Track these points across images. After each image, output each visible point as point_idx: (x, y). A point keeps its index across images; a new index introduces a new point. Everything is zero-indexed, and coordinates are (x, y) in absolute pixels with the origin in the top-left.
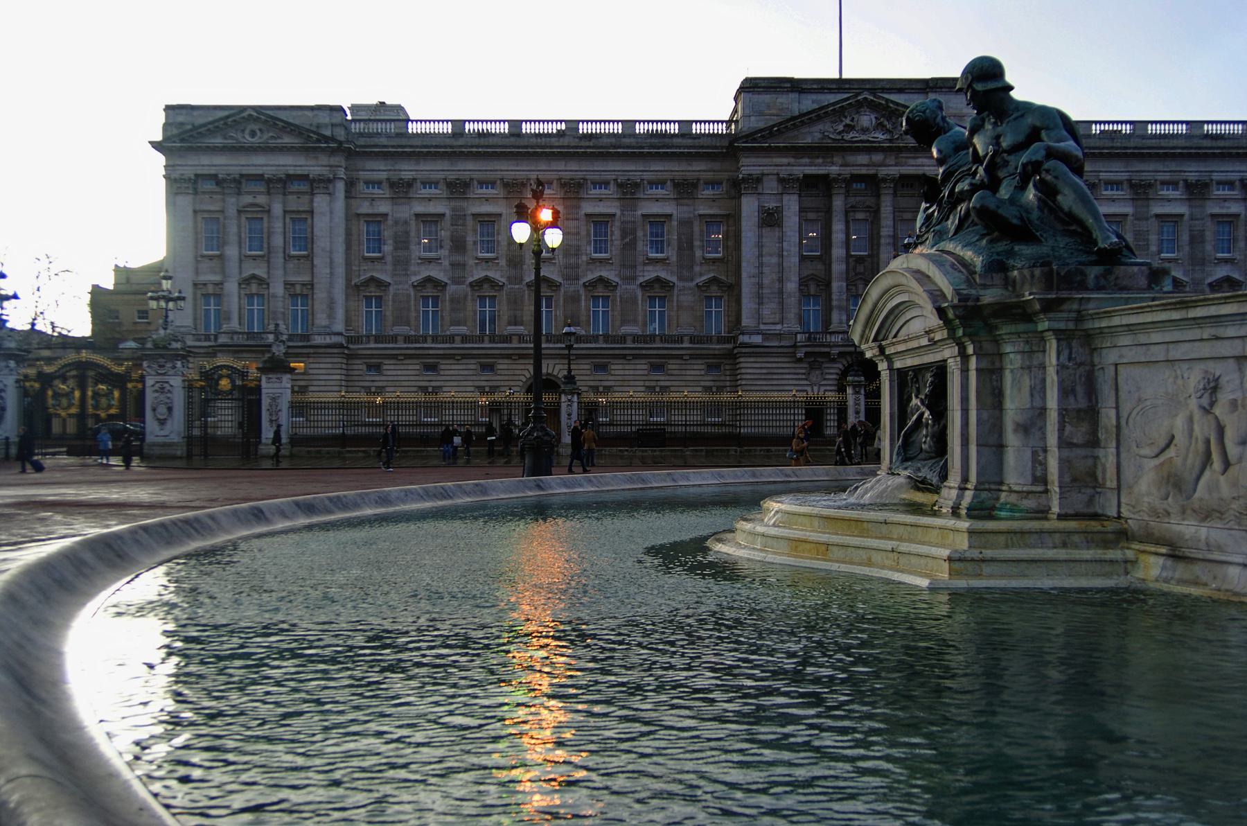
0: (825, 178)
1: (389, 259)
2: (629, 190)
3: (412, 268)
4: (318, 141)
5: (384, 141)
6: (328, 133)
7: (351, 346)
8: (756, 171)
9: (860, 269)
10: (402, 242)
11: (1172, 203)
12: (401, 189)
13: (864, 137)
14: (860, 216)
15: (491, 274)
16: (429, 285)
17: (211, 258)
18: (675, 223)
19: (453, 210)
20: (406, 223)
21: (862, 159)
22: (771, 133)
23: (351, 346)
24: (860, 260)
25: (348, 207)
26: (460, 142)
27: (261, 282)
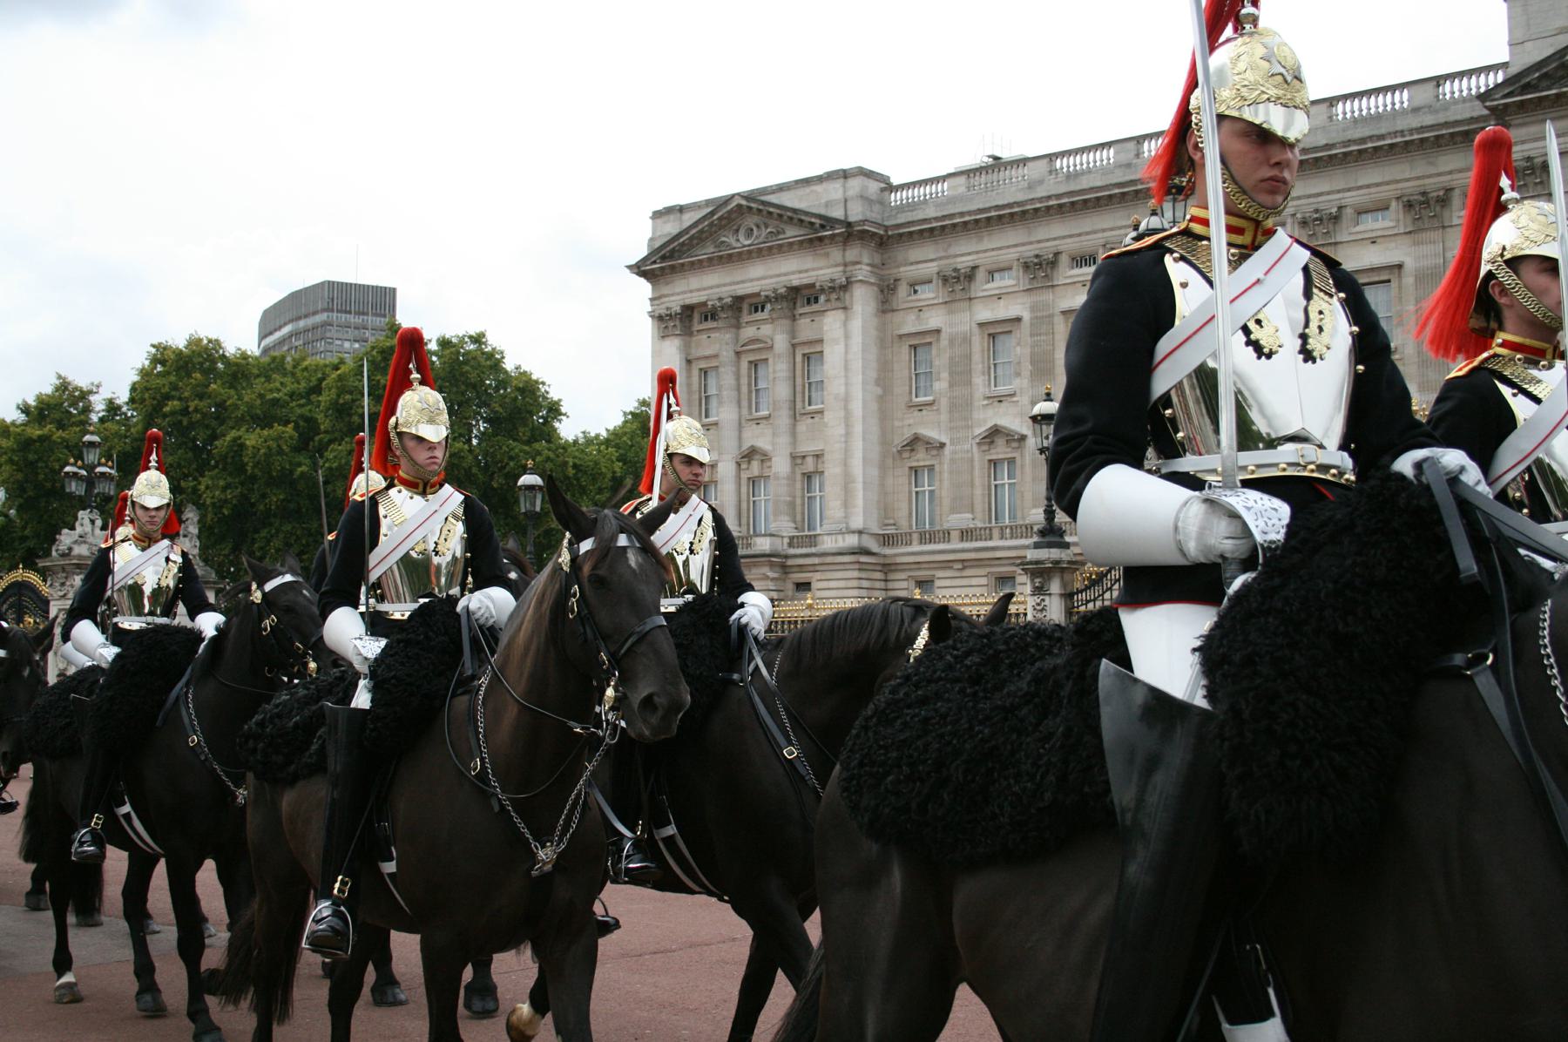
1: (944, 403)
3: (976, 415)
4: (823, 227)
5: (931, 212)
6: (837, 213)
7: (888, 551)
10: (961, 374)
12: (959, 282)
16: (1000, 441)
18: (1409, 280)
19: (1033, 309)
20: (966, 340)
23: (888, 551)
25: (882, 328)
26: (1041, 192)
27: (765, 458)
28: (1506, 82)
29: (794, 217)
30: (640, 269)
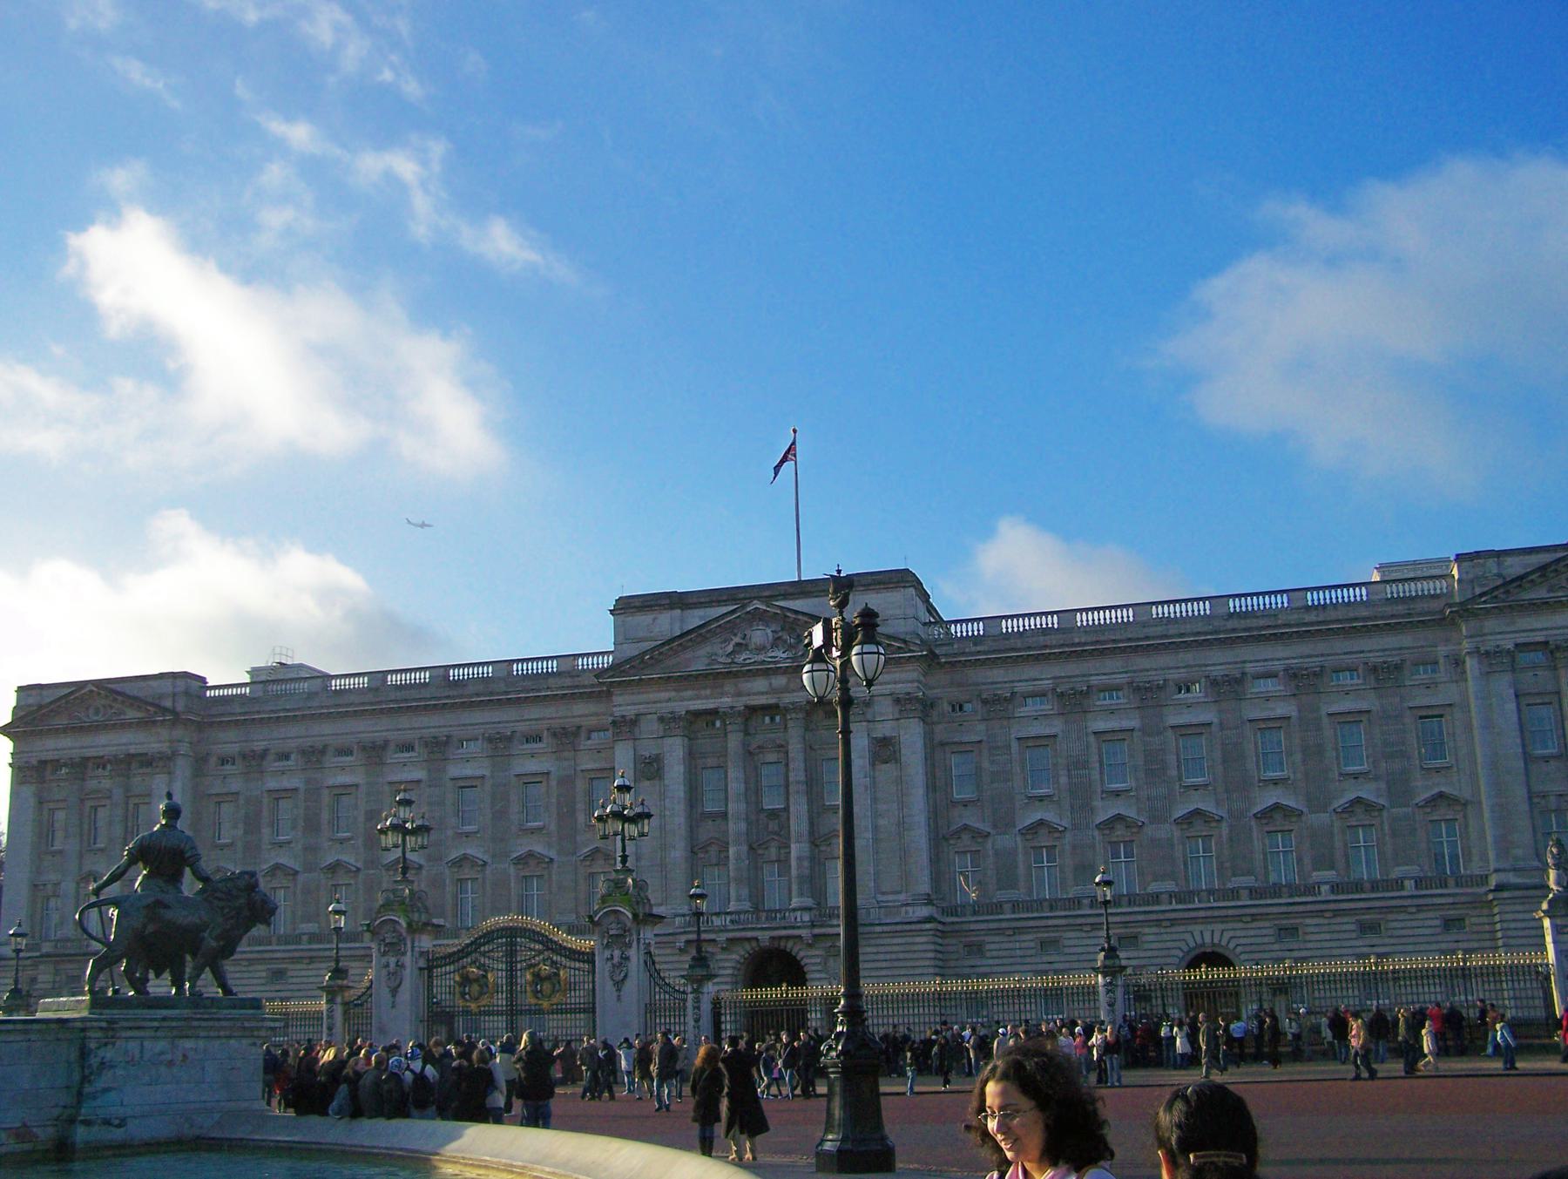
0: (714, 713)
1: (239, 844)
2: (500, 743)
6: (168, 704)
8: (630, 711)
9: (773, 826)
11: (1195, 708)
13: (761, 657)
14: (772, 757)
15: (345, 858)
17: (54, 854)
18: (554, 783)
19: (308, 781)
21: (760, 684)
22: (643, 661)
24: (773, 814)
28: (611, 668)
29: (136, 702)
30: (6, 730)
